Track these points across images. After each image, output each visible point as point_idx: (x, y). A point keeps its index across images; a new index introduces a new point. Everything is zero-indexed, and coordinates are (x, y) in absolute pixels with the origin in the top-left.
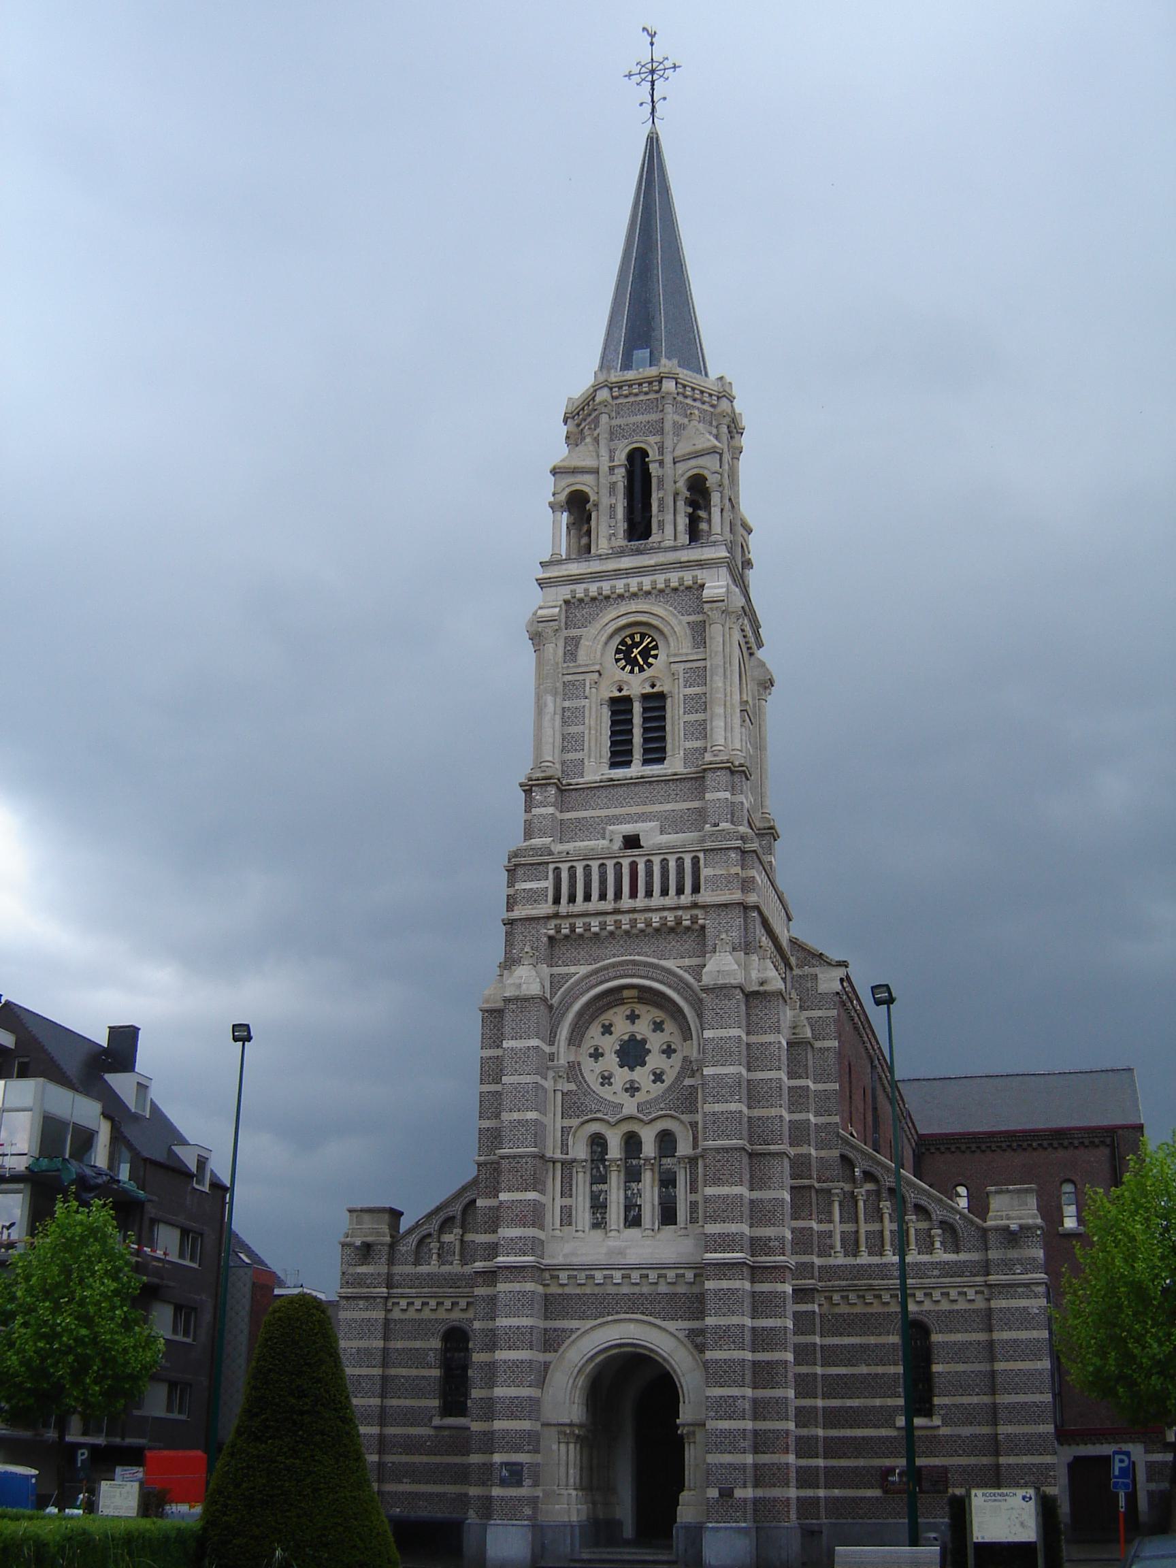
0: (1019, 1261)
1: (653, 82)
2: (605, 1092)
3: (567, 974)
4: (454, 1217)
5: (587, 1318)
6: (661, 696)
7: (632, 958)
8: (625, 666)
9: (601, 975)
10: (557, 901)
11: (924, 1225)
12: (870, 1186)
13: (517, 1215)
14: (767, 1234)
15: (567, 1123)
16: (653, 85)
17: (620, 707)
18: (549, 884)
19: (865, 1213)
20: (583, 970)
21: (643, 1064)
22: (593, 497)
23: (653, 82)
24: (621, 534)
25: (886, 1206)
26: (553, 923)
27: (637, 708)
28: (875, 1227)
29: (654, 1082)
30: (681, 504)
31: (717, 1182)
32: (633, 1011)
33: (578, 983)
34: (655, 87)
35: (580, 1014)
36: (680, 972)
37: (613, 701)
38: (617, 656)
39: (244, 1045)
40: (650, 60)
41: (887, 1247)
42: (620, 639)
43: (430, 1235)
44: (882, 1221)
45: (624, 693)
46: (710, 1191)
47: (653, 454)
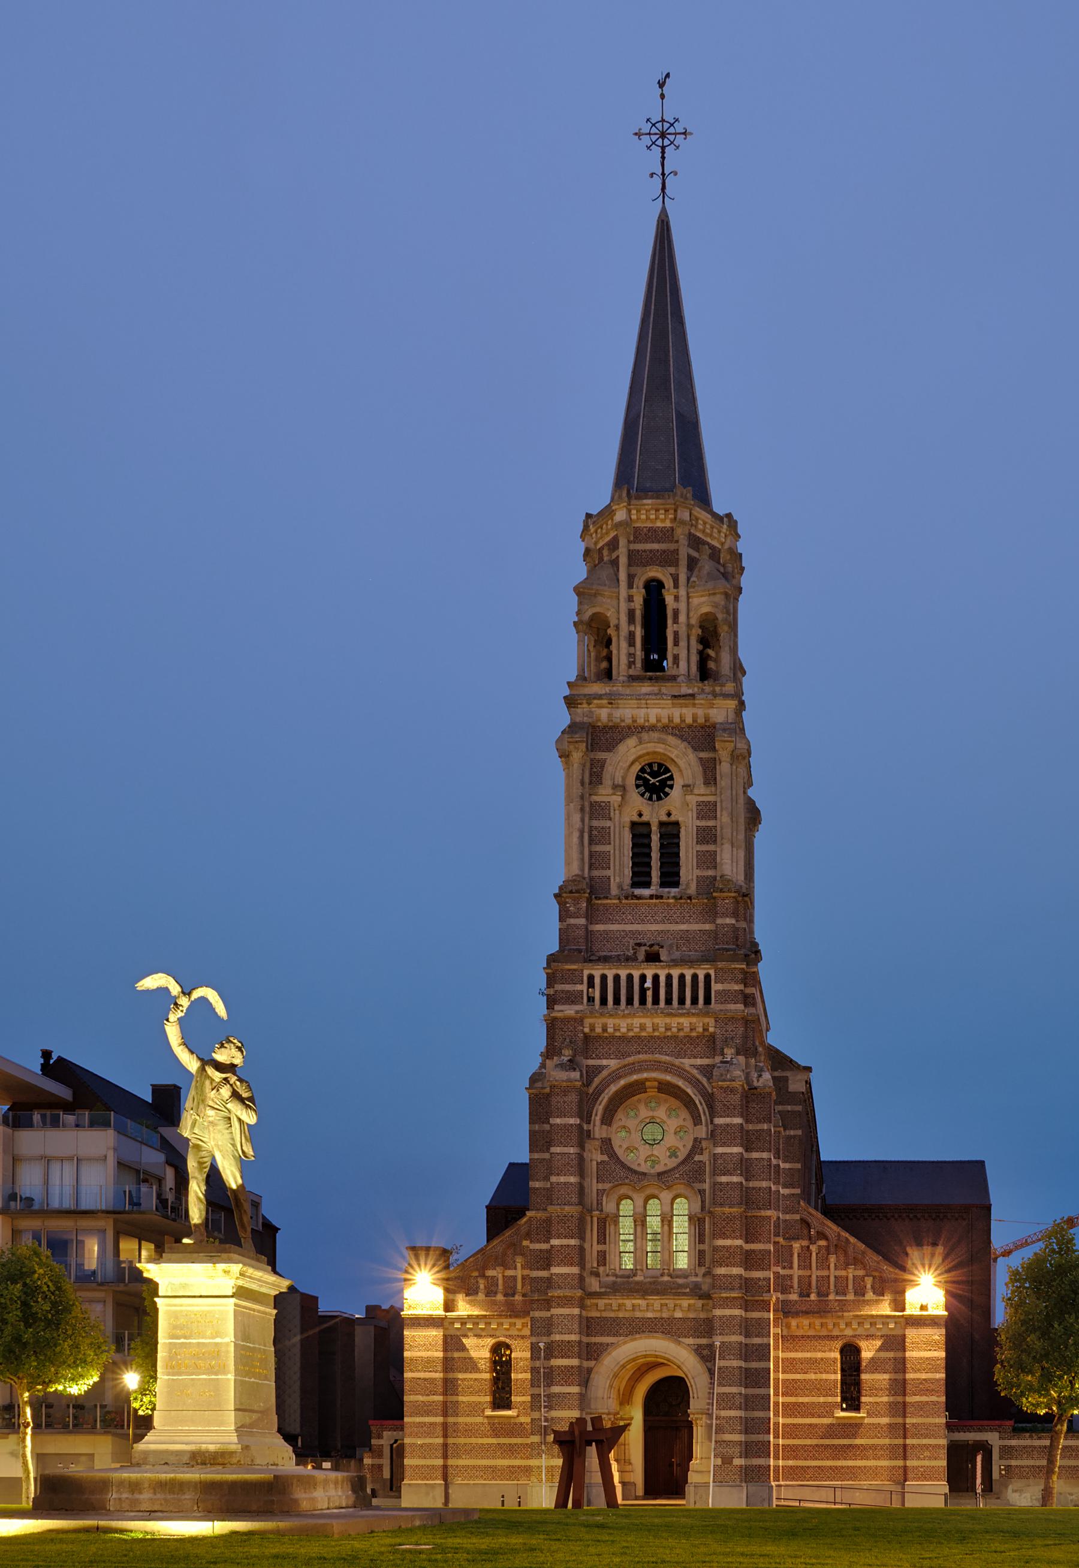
1: (663, 148)
6: (677, 824)
8: (644, 793)
11: (861, 1273)
13: (565, 1257)
14: (757, 1276)
15: (601, 1186)
16: (663, 152)
17: (640, 832)
19: (817, 1263)
22: (613, 622)
23: (663, 148)
24: (639, 664)
25: (832, 1259)
31: (724, 1236)
34: (665, 155)
35: (611, 1100)
36: (695, 1072)
37: (634, 824)
40: (660, 119)
46: (720, 1242)
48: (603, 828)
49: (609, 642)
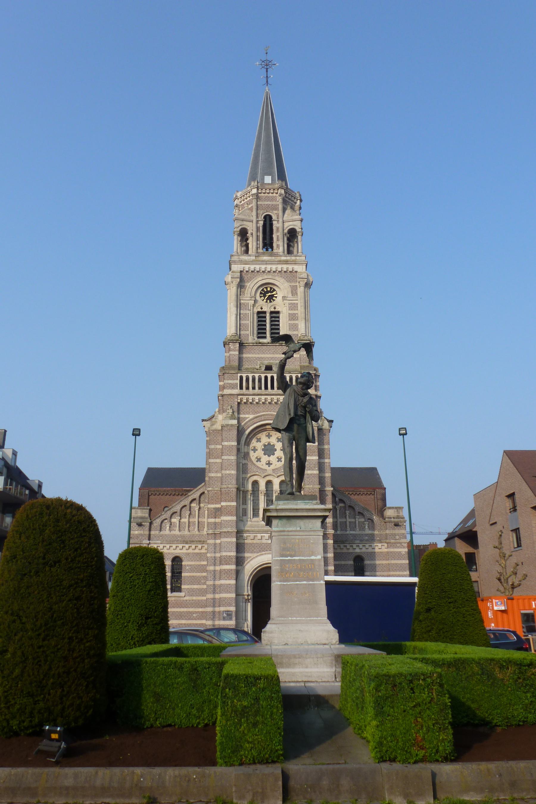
0: (398, 534)
1: (267, 69)
2: (258, 464)
3: (245, 418)
4: (176, 512)
5: (254, 552)
6: (278, 312)
7: (271, 413)
9: (258, 419)
10: (241, 388)
11: (363, 520)
12: (342, 505)
13: (229, 511)
17: (261, 315)
18: (238, 382)
20: (251, 416)
21: (274, 454)
23: (267, 69)
25: (348, 512)
26: (240, 397)
27: (268, 316)
28: (344, 520)
29: (278, 461)
30: (286, 239)
32: (269, 434)
33: (249, 421)
37: (259, 313)
38: (261, 295)
39: (136, 437)
41: (348, 528)
42: (262, 289)
43: (166, 519)
44: (346, 517)
45: (263, 310)
47: (274, 217)
48: (245, 314)
49: (247, 239)
